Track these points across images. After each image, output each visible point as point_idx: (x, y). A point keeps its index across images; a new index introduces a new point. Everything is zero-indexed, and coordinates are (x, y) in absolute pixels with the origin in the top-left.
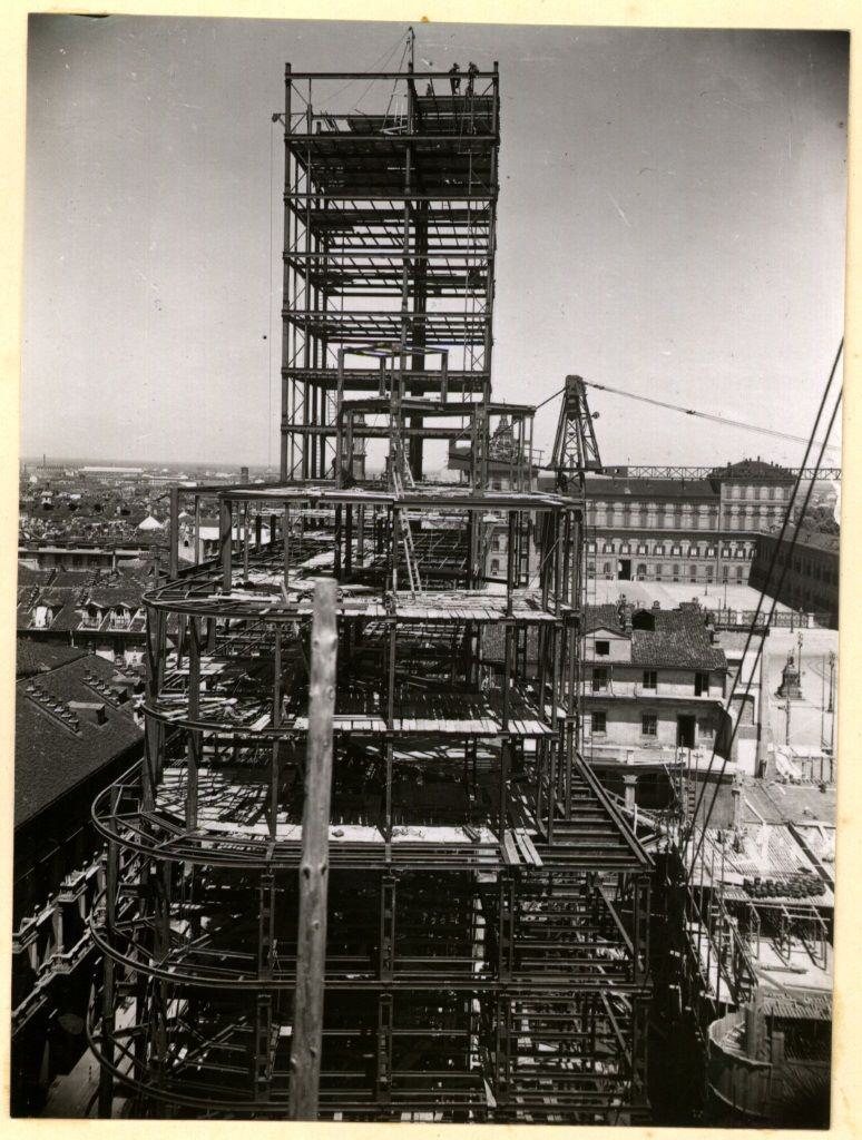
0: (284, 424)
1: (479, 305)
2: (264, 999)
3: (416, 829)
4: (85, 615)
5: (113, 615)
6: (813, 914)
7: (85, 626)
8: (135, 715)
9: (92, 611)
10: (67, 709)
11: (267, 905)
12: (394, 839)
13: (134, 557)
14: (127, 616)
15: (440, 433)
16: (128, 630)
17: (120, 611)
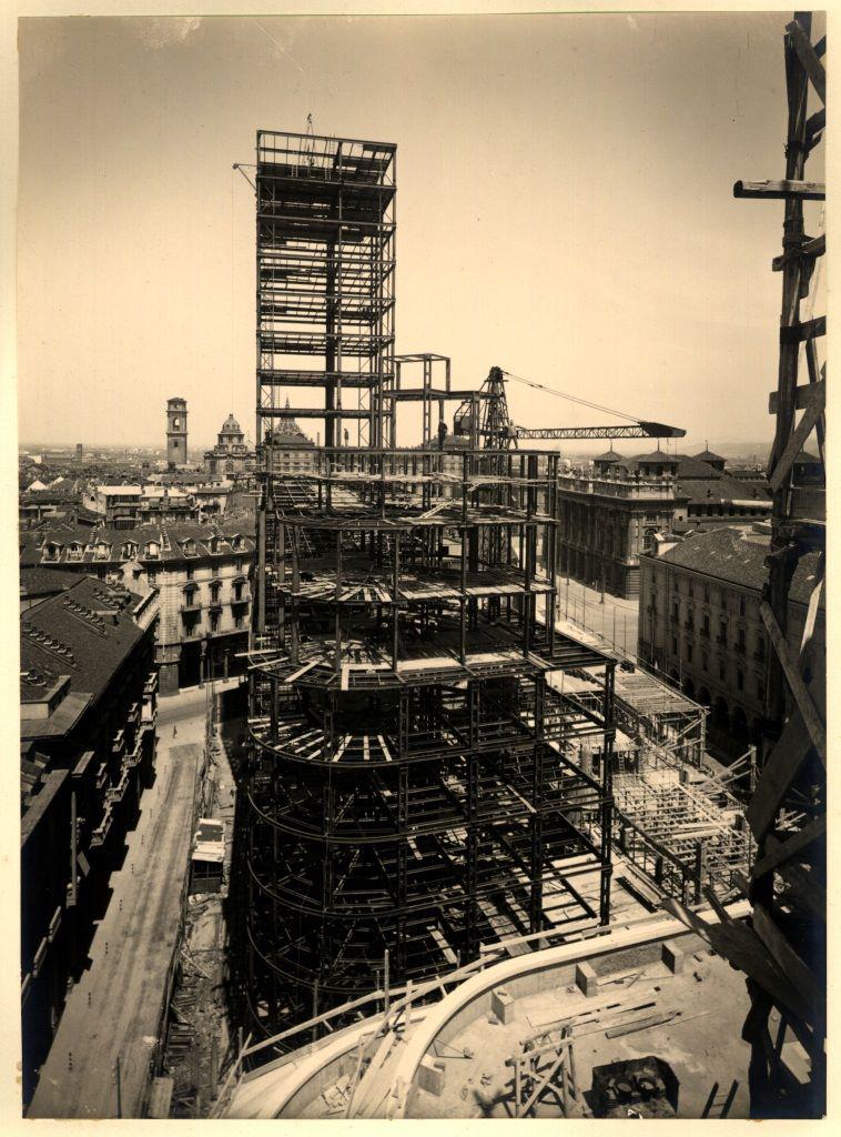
0: (259, 407)
1: (266, 326)
2: (405, 770)
3: (477, 656)
4: (46, 551)
5: (69, 551)
6: (589, 696)
7: (47, 559)
8: (134, 618)
9: (52, 548)
10: (96, 616)
11: (404, 711)
12: (468, 663)
13: (50, 510)
14: (79, 550)
15: (315, 413)
16: (82, 561)
17: (74, 547)
